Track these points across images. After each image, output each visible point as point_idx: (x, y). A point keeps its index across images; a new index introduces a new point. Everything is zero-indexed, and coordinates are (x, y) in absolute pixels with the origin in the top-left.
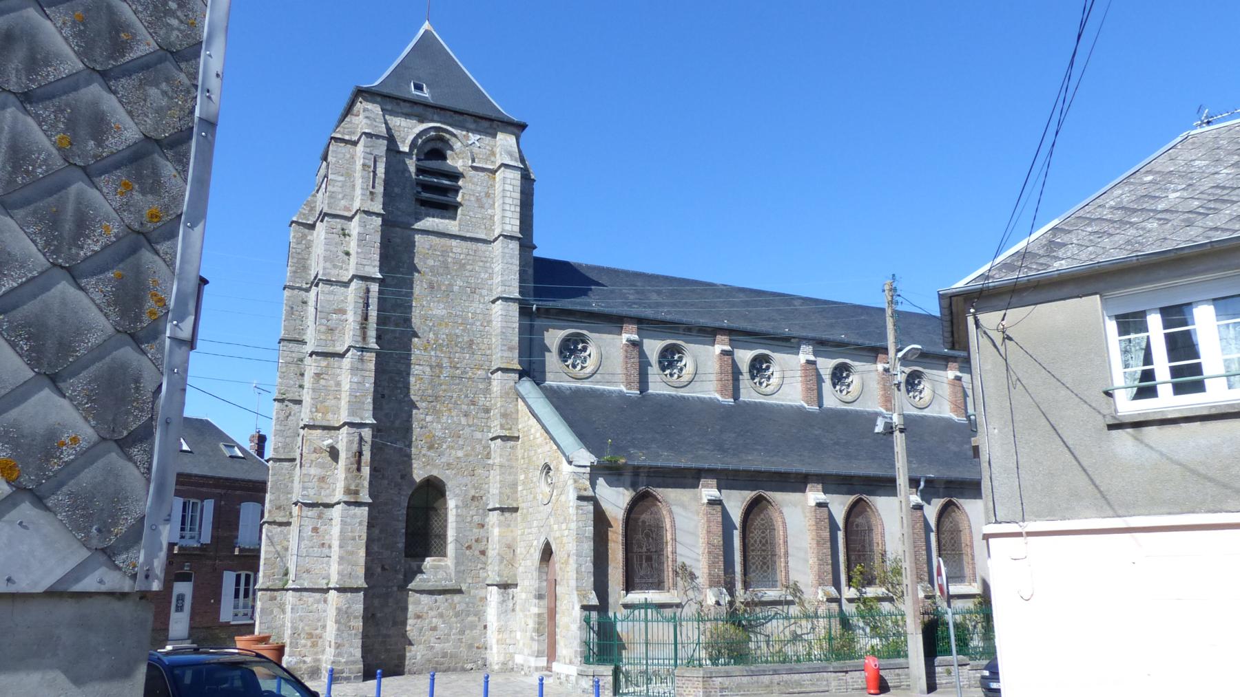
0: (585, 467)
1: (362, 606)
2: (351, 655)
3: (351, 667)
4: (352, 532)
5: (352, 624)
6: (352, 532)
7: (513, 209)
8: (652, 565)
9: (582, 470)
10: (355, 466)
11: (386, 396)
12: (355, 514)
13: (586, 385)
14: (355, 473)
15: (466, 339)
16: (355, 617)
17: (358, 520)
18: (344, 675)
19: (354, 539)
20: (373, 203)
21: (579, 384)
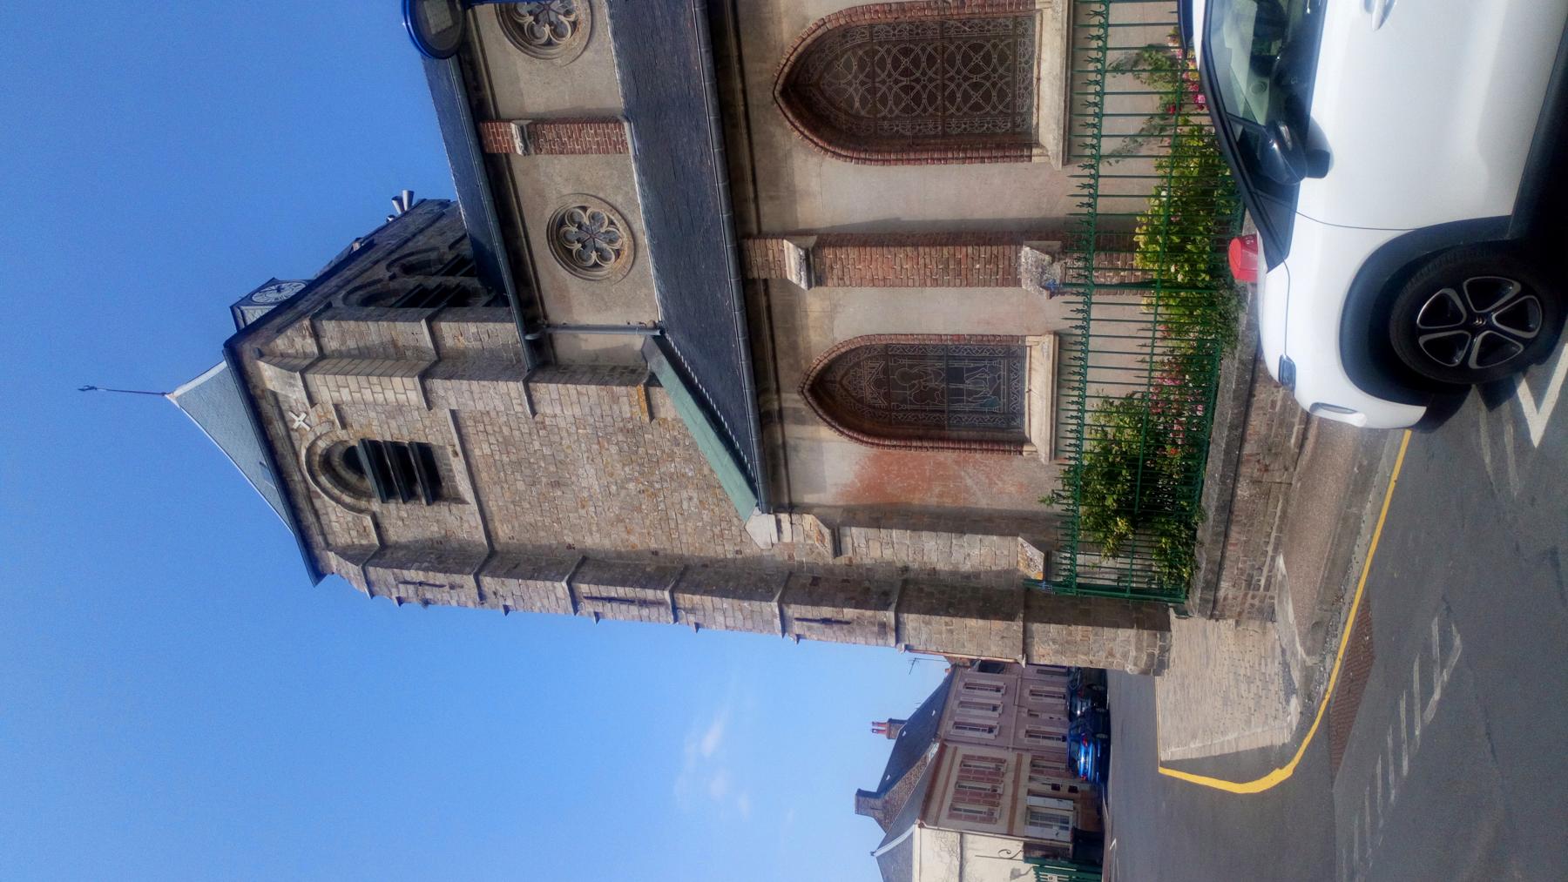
0: (778, 522)
1: (1052, 626)
2: (1128, 641)
3: (1145, 644)
4: (941, 633)
5: (1079, 638)
6: (941, 633)
7: (378, 389)
8: (969, 370)
9: (786, 525)
10: (845, 626)
11: (737, 548)
12: (915, 629)
13: (640, 224)
14: (855, 625)
15: (621, 437)
16: (1070, 634)
17: (923, 625)
18: (1157, 652)
19: (951, 632)
20: (466, 586)
21: (644, 240)
